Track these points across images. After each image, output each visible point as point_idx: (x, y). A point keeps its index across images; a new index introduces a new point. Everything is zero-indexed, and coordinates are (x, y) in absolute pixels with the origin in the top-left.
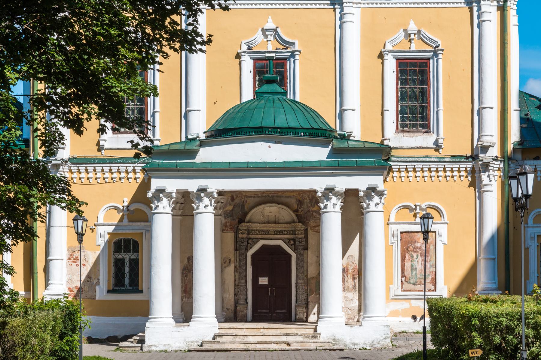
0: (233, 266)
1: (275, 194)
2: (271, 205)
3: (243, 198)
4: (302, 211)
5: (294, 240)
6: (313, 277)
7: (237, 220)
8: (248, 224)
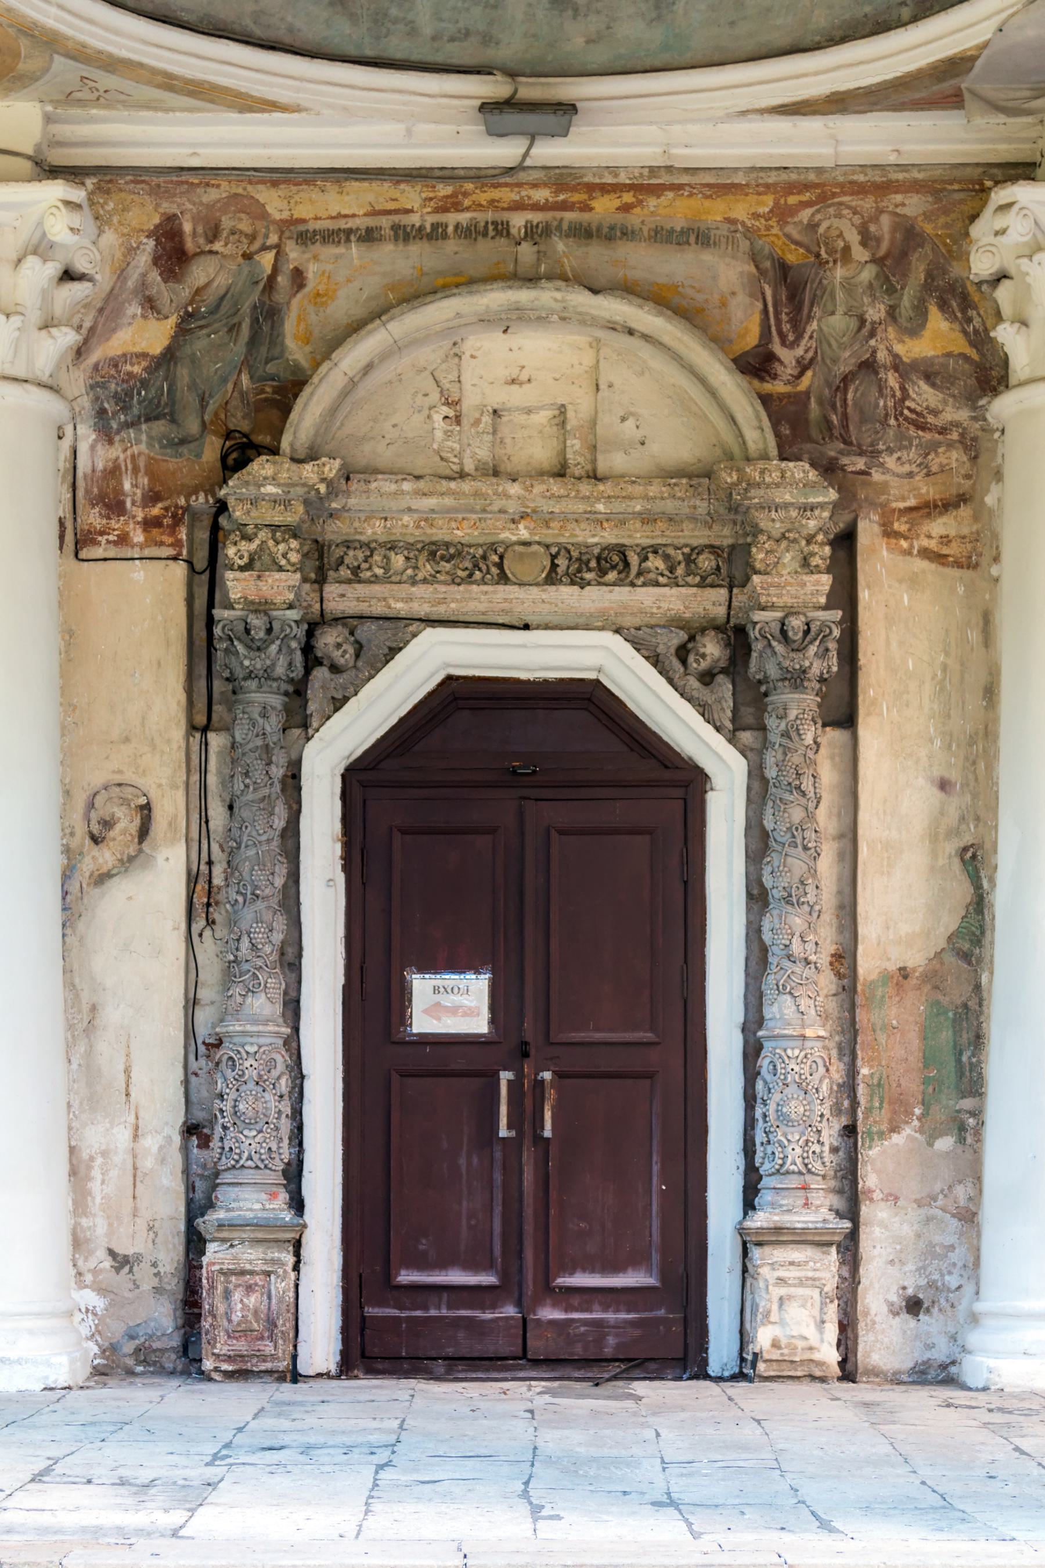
1: (564, 206)
2: (524, 296)
3: (264, 248)
4: (803, 367)
6: (904, 973)
7: (211, 450)
8: (309, 472)
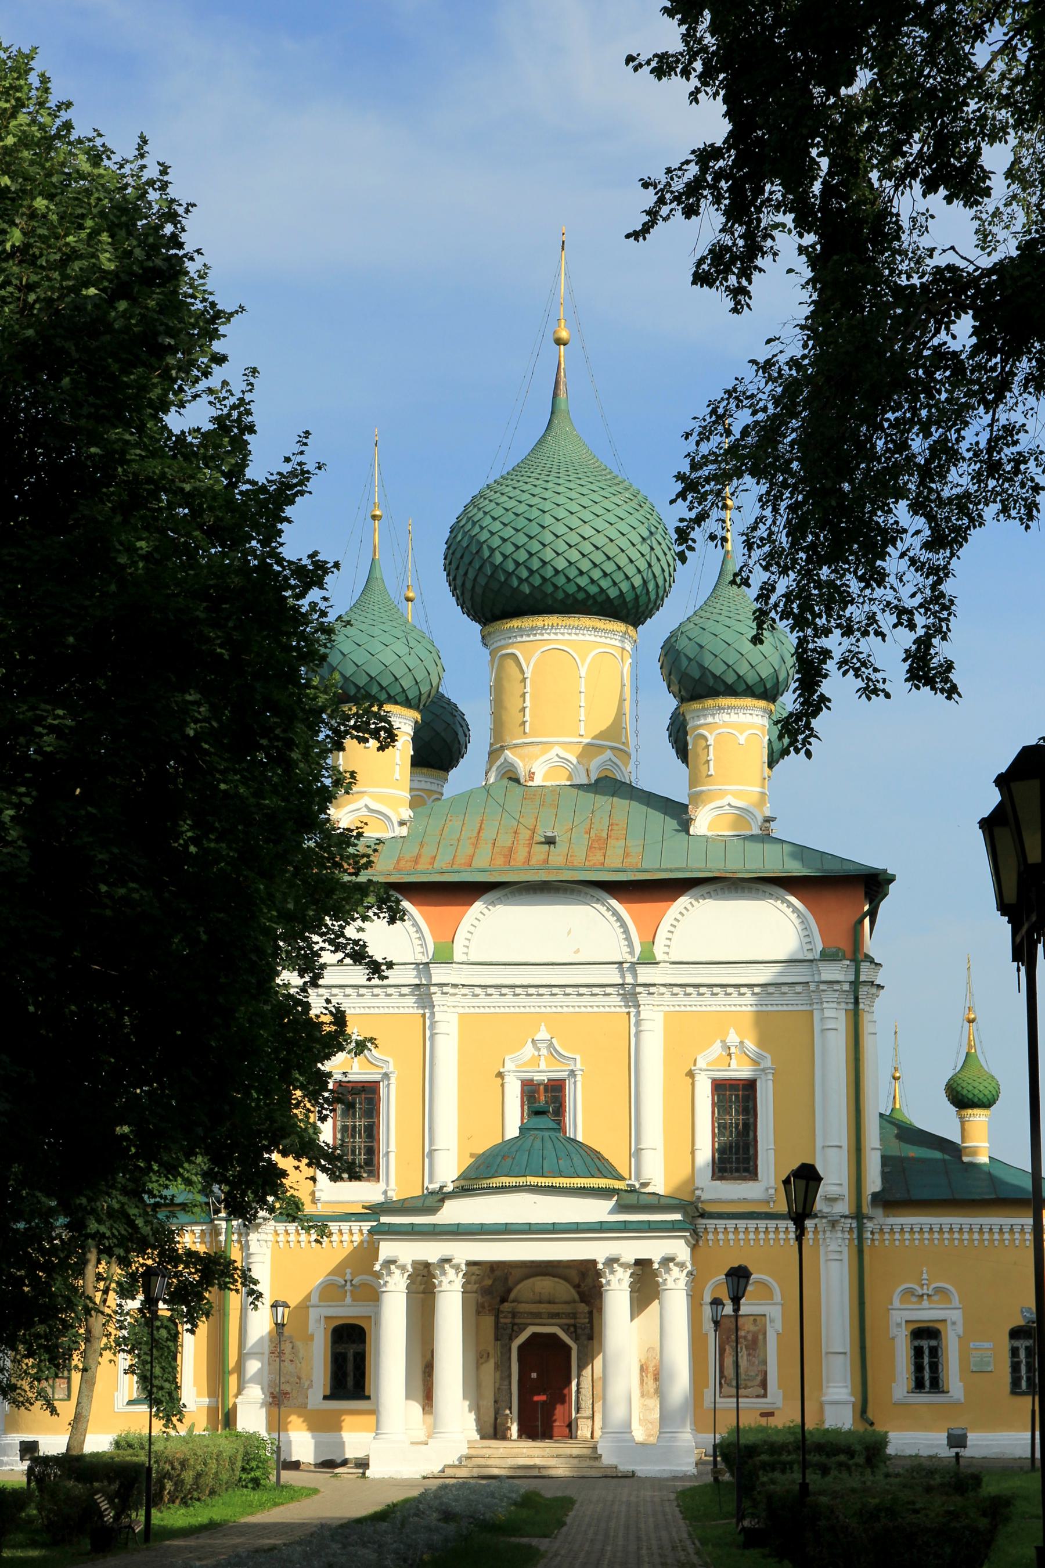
0: (491, 1364)
5: (575, 1326)
7: (498, 1299)
